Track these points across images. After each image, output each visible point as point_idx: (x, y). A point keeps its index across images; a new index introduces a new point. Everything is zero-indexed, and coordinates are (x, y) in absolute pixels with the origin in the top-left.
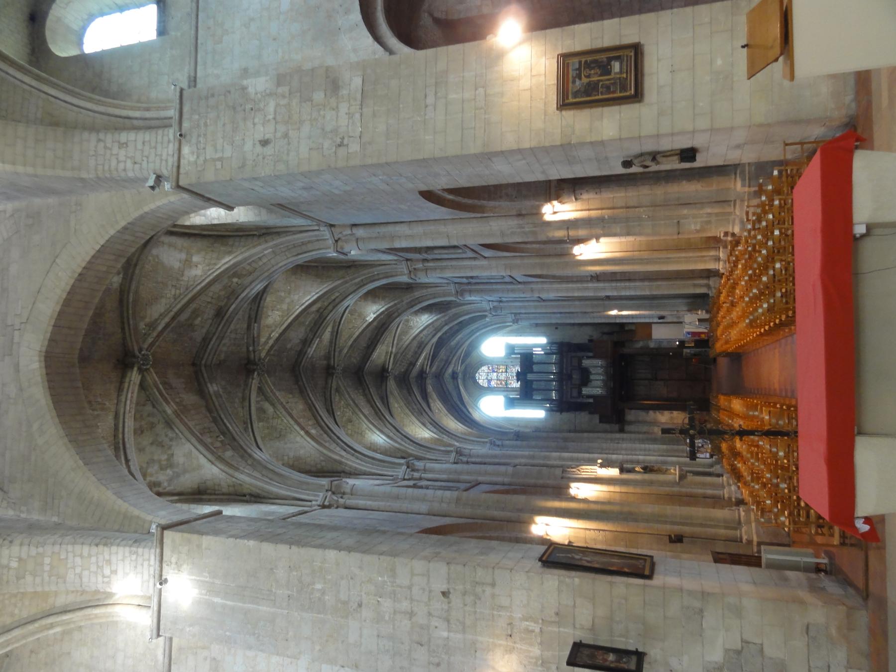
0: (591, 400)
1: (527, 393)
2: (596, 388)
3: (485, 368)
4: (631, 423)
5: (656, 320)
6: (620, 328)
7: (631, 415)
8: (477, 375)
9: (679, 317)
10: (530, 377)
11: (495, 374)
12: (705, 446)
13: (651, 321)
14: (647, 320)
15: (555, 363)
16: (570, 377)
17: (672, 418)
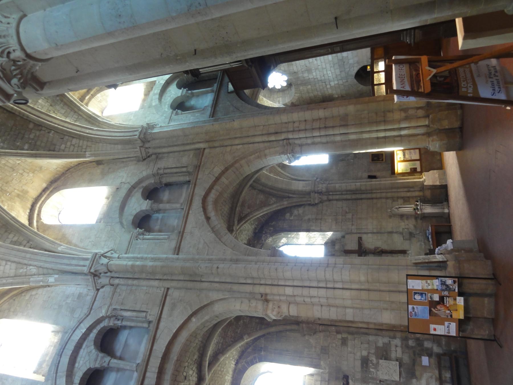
12: (449, 302)
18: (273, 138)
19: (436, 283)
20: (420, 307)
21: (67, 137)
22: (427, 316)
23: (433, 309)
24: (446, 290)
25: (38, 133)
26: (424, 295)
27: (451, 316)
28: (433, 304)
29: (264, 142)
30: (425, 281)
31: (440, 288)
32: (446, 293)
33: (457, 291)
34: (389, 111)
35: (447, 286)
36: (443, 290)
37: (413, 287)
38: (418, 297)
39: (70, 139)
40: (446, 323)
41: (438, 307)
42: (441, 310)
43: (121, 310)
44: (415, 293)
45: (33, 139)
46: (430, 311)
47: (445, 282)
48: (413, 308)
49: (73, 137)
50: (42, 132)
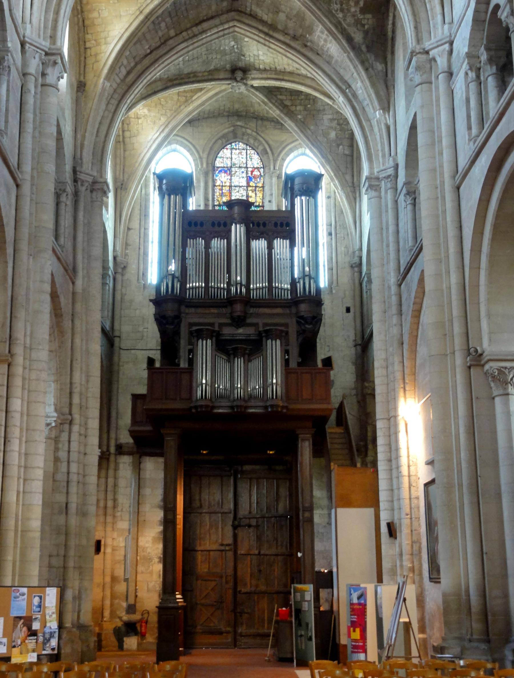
0: (184, 364)
1: (195, 228)
2: (213, 377)
3: (255, 161)
4: (138, 468)
5: (384, 517)
6: (354, 440)
7: (154, 469)
8: (241, 145)
9: (393, 572)
10: (238, 231)
11: (244, 183)
12: (31, 642)
13: (383, 505)
14: (383, 496)
15: (270, 287)
16: (239, 322)
17: (148, 560)
18: (76, 400)
19: (53, 625)
20: (24, 603)
21: (132, 64)
22: (14, 613)
23: (22, 621)
24: (45, 639)
25: (160, 34)
26: (38, 609)
27: (14, 647)
28: (28, 621)
29: (71, 384)
30: (54, 611)
31: (47, 630)
32: (41, 639)
33: (44, 652)
34: (80, 574)
35: (49, 640)
36: (44, 633)
37: (48, 595)
38: (36, 601)
39: (128, 68)
40: (5, 640)
41: (25, 629)
42: (21, 632)
43: (8, 81)
44: (41, 597)
45: (159, 23)
46: (20, 618)
47: (53, 637)
48: (23, 594)
49: (128, 73)
50: (157, 39)
